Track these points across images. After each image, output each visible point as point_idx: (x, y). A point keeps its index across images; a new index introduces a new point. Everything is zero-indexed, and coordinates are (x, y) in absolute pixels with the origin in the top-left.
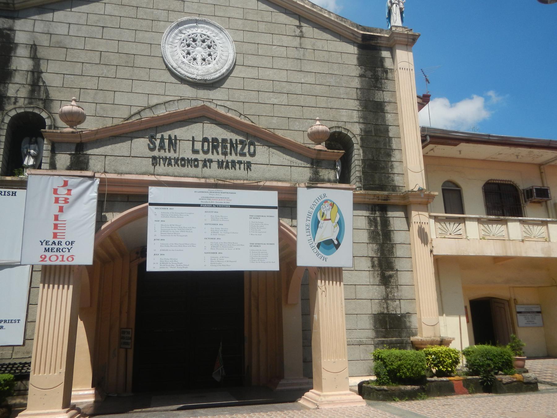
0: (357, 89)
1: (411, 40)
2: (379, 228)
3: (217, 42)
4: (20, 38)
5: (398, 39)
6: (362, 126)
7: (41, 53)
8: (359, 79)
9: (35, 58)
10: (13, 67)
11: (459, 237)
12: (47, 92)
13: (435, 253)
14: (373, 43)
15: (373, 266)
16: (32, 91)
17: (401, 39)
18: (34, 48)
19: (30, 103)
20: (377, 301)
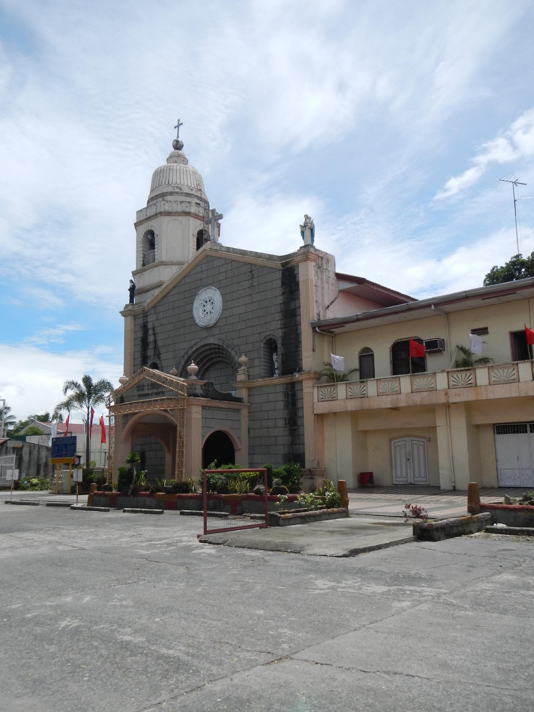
0: (281, 304)
1: (305, 257)
2: (290, 399)
3: (214, 299)
4: (150, 325)
5: (297, 260)
6: (283, 330)
7: (157, 330)
8: (282, 296)
9: (154, 334)
10: (149, 341)
11: (334, 399)
12: (159, 351)
13: (315, 413)
14: (289, 266)
15: (285, 424)
16: (155, 351)
17: (299, 259)
18: (154, 329)
19: (154, 358)
20: (287, 446)
